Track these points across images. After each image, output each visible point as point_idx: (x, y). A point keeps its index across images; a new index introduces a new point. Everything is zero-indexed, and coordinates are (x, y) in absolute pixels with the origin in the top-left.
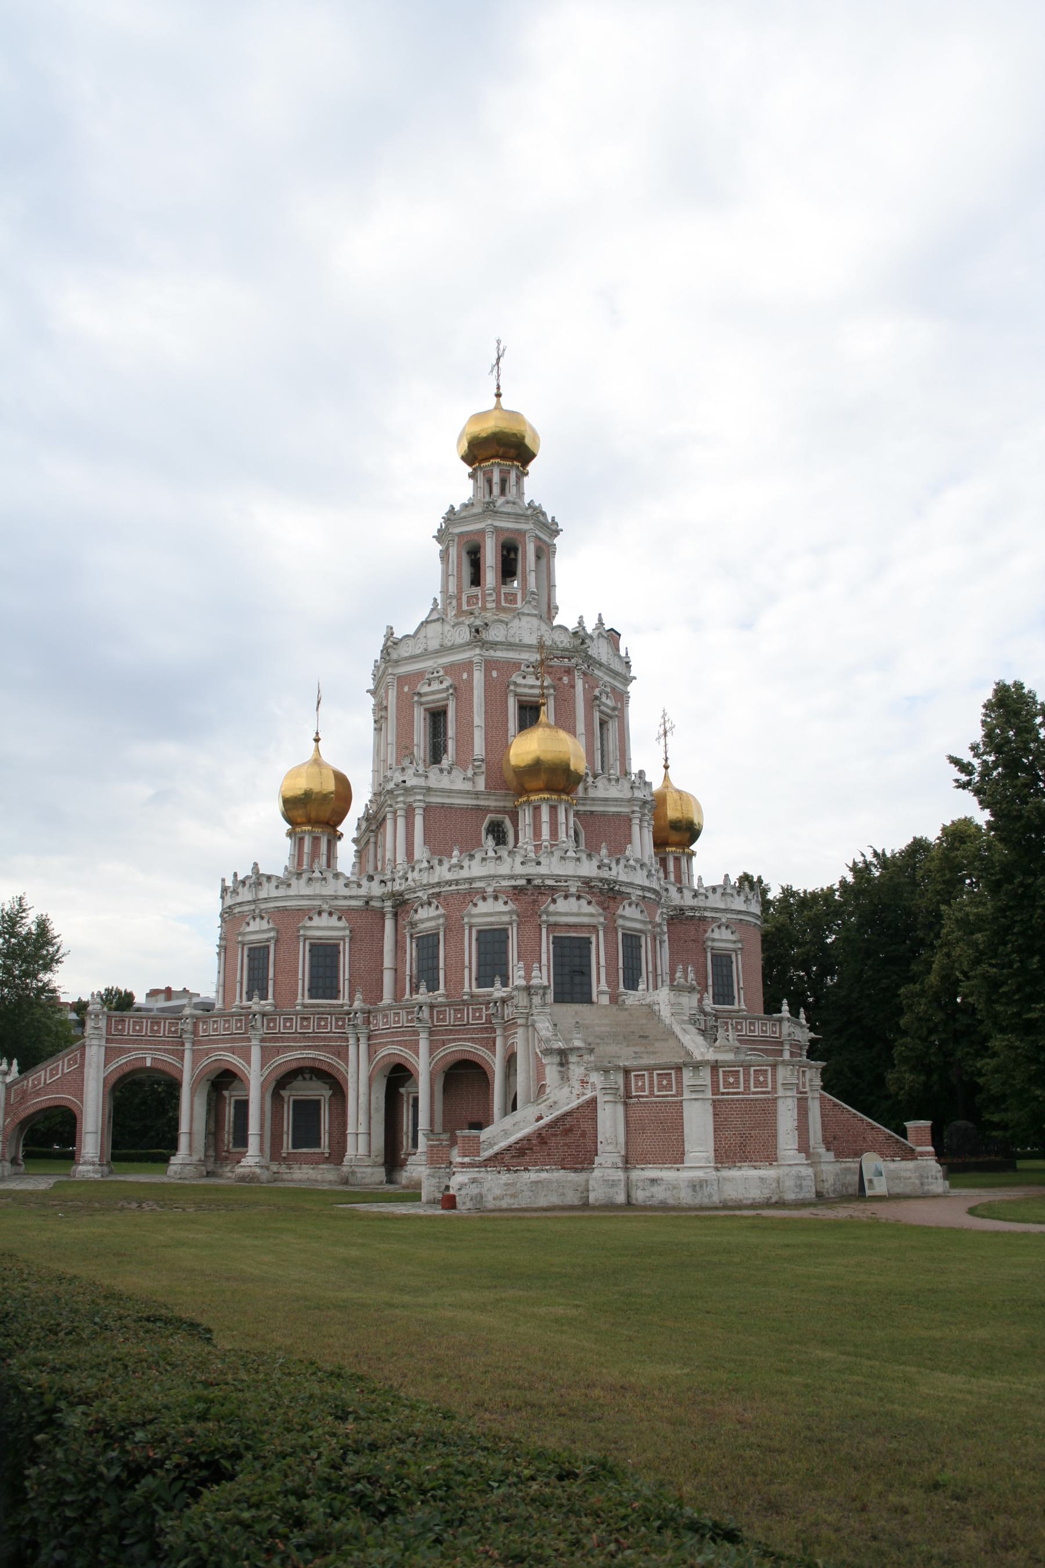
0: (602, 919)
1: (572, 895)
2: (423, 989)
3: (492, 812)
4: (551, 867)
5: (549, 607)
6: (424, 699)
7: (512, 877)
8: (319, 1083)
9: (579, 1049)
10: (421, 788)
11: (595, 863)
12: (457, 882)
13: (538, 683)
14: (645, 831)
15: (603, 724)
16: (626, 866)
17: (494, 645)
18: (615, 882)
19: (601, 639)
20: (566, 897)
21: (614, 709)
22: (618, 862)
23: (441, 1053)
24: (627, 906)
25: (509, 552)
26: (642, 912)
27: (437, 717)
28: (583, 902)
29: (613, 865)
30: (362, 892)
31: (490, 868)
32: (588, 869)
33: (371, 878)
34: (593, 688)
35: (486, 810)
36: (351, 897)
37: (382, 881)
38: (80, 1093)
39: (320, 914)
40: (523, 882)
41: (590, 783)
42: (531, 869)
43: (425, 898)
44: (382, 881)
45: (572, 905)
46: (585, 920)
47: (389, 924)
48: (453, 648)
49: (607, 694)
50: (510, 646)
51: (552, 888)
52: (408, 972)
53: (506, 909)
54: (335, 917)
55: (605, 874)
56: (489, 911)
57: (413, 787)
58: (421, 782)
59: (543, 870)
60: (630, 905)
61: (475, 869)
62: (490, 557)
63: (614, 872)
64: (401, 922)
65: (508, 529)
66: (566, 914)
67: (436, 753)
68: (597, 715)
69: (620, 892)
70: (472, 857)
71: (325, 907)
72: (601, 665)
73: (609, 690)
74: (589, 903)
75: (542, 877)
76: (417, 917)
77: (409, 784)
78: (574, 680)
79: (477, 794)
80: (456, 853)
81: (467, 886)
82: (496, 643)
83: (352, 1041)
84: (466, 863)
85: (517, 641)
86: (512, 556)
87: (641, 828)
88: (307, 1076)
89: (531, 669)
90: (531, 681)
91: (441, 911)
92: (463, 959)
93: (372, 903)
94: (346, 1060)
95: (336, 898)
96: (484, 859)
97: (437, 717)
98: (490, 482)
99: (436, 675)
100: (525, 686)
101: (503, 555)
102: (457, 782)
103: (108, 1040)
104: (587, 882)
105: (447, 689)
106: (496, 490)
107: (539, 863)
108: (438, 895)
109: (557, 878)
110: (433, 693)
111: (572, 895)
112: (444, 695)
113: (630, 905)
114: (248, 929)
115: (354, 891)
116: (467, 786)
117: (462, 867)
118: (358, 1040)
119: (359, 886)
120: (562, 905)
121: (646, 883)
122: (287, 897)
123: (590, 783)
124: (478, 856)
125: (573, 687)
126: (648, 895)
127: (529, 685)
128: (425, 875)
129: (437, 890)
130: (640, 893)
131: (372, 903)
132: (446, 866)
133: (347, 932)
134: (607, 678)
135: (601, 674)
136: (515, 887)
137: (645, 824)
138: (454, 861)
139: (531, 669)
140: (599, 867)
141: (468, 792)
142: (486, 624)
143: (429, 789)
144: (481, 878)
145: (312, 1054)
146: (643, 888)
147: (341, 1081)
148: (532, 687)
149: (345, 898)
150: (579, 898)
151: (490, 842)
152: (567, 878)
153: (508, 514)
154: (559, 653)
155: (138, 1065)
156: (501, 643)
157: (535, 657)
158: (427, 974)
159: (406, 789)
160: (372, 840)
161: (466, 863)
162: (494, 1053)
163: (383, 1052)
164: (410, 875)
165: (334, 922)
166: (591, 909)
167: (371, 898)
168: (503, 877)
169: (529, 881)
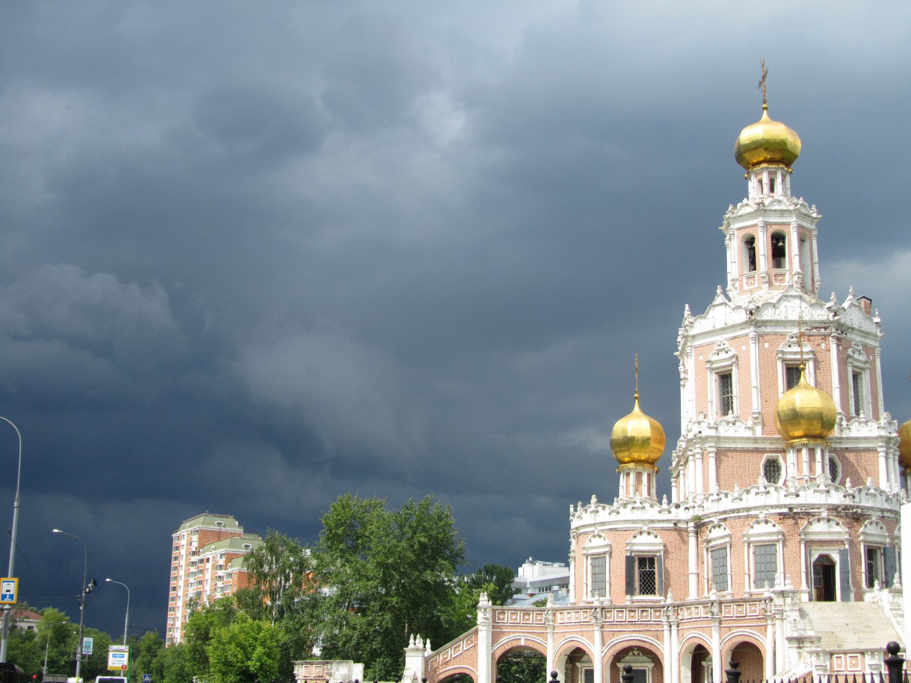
0: (847, 536)
1: (823, 519)
2: (714, 591)
3: (768, 452)
4: (809, 498)
5: (813, 280)
6: (714, 366)
7: (778, 507)
8: (645, 658)
9: (810, 637)
10: (713, 437)
11: (841, 494)
12: (738, 510)
13: (799, 350)
14: (891, 461)
15: (856, 376)
16: (867, 494)
17: (765, 323)
19: (853, 308)
20: (819, 520)
21: (866, 362)
22: (860, 490)
23: (727, 636)
25: (778, 242)
26: (882, 528)
27: (725, 379)
29: (857, 495)
30: (671, 517)
31: (761, 500)
32: (836, 498)
33: (678, 506)
34: (846, 349)
35: (763, 451)
36: (663, 521)
37: (686, 508)
38: (475, 662)
39: (641, 533)
40: (785, 510)
41: (845, 426)
42: (792, 501)
43: (716, 522)
44: (686, 508)
46: (835, 537)
47: (692, 540)
48: (734, 327)
49: (859, 351)
50: (778, 323)
52: (706, 577)
53: (775, 530)
54: (652, 536)
56: (763, 531)
57: (707, 437)
58: (712, 433)
59: (801, 500)
60: (871, 523)
61: (751, 500)
62: (763, 247)
63: (857, 499)
64: (700, 539)
66: (819, 533)
67: (726, 405)
68: (850, 370)
69: (862, 515)
70: (748, 492)
71: (645, 528)
72: (853, 329)
73: (860, 348)
74: (838, 524)
75: (801, 506)
76: (711, 536)
77: (703, 435)
79: (756, 440)
80: (737, 489)
81: (745, 514)
82: (766, 322)
83: (666, 627)
84: (744, 496)
85: (783, 319)
86: (780, 244)
87: (887, 459)
88: (636, 653)
89: (795, 339)
90: (795, 349)
91: (728, 532)
92: (744, 568)
93: (679, 525)
94: (662, 641)
95: (653, 521)
96: (757, 493)
97: (725, 379)
98: (761, 182)
99: (722, 347)
100: (790, 353)
101: (773, 244)
102: (740, 431)
103: (493, 627)
104: (834, 509)
105: (731, 358)
106: (766, 188)
107: (798, 496)
108: (725, 519)
109: (812, 506)
110: (721, 361)
112: (729, 363)
113: (871, 523)
114: (590, 545)
115: (665, 516)
116: (749, 434)
117: (741, 500)
118: (670, 626)
119: (670, 512)
121: (886, 506)
122: (617, 522)
123: (845, 426)
124: (753, 491)
125: (829, 350)
126: (886, 514)
127: (793, 352)
128: (716, 504)
129: (724, 516)
130: (880, 514)
131: (679, 525)
132: (730, 498)
133: (662, 547)
134: (858, 339)
135: (853, 336)
136: (780, 514)
137: (891, 455)
138: (736, 495)
139: (795, 339)
140: (845, 496)
141: (748, 438)
142: (758, 307)
143: (719, 437)
144: (755, 508)
145: (638, 636)
146: (882, 511)
147: (660, 657)
148: (796, 353)
149: (659, 521)
150: (829, 520)
151: (762, 481)
152: (819, 506)
153: (775, 211)
154: (817, 325)
155: (515, 644)
156: (770, 321)
157: (796, 331)
158: (720, 579)
159: (701, 438)
160: (682, 472)
161: (744, 496)
162: (765, 636)
163: (688, 635)
164: (705, 504)
165: (651, 539)
167: (679, 521)
168: (772, 507)
169: (791, 509)
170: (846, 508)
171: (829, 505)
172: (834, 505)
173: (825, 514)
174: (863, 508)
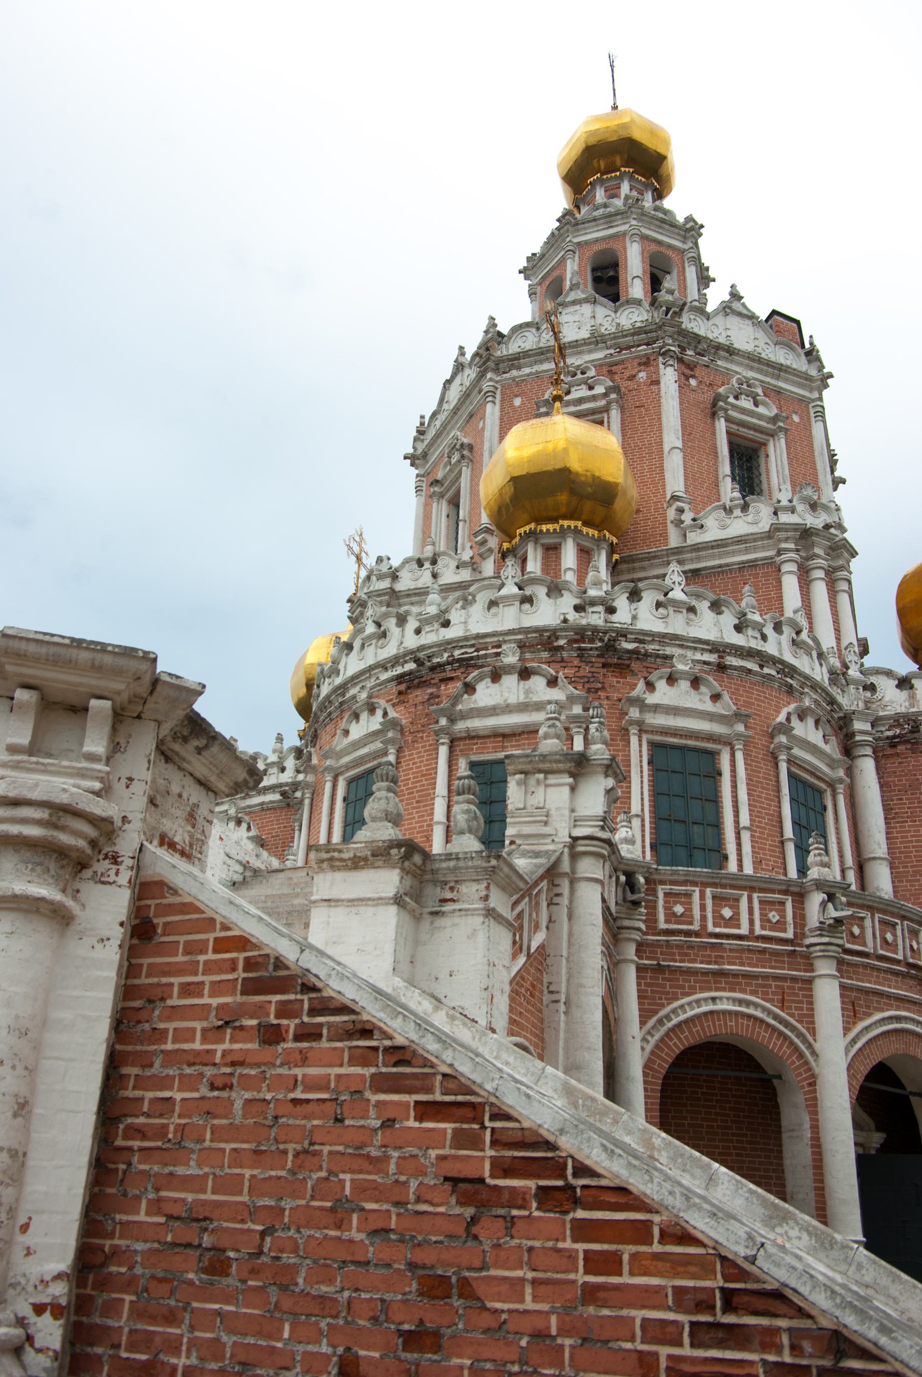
1: (509, 669)
18: (623, 634)
20: (496, 677)
21: (774, 420)
24: (661, 685)
28: (538, 683)
45: (511, 689)
51: (466, 664)
55: (595, 618)
65: (597, 240)
66: (493, 711)
74: (552, 682)
78: (657, 372)
104: (543, 641)
107: (446, 624)
111: (509, 669)
120: (487, 694)
121: (738, 640)
136: (400, 679)
150: (525, 674)
152: (498, 639)
166: (557, 694)
170: (582, 634)
171: (526, 631)
172: (539, 630)
173: (511, 658)
174: (643, 637)
